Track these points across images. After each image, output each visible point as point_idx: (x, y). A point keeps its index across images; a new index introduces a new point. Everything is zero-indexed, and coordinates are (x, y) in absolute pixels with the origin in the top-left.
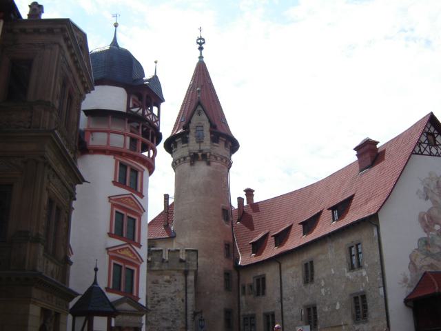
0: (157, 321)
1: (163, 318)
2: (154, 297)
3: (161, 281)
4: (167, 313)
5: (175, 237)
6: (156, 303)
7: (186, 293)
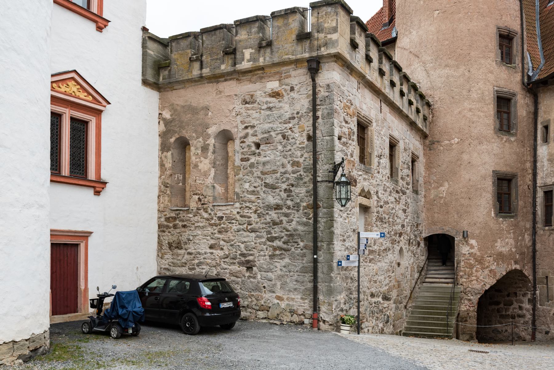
0: (253, 193)
1: (267, 185)
2: (246, 136)
3: (260, 97)
4: (275, 172)
6: (253, 148)
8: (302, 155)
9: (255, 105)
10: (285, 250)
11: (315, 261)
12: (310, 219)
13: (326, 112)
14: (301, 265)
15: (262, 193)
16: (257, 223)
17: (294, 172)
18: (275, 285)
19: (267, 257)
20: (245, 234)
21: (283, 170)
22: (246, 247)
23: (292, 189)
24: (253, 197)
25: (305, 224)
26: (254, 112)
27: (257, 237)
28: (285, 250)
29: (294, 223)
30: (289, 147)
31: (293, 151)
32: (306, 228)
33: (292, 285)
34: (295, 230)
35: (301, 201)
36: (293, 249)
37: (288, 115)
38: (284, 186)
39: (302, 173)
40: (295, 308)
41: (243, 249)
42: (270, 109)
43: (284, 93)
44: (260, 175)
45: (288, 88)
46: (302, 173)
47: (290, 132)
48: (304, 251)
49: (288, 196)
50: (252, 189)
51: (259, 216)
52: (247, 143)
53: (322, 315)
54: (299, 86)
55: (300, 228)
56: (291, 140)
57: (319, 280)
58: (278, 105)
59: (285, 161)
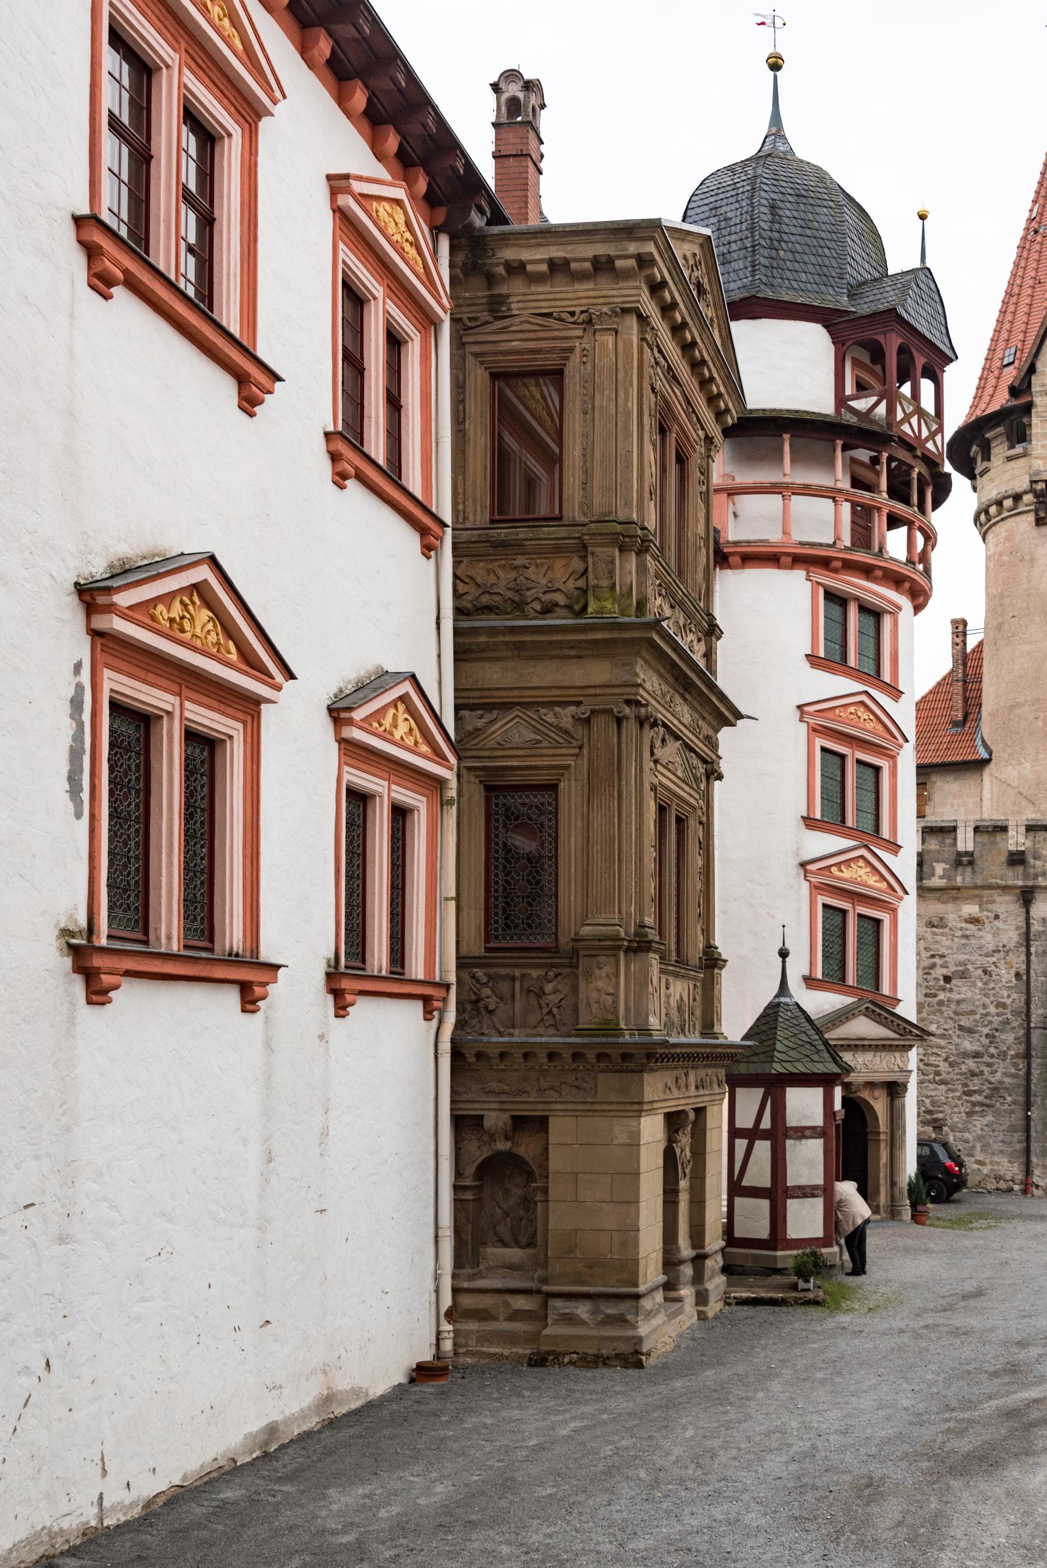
0: (943, 1036)
1: (961, 1028)
2: (933, 966)
3: (952, 919)
4: (972, 1012)
5: (988, 761)
6: (942, 983)
7: (1028, 954)
8: (1009, 996)
9: (946, 930)
10: (988, 1106)
11: (1028, 1119)
12: (1020, 1070)
13: (1041, 949)
14: (1008, 1123)
15: (956, 1039)
16: (948, 1073)
17: (998, 1015)
18: (973, 1147)
19: (963, 1115)
20: (932, 1086)
21: (984, 1012)
22: (933, 1103)
23: (997, 1034)
24: (942, 1042)
25: (1014, 1076)
26: (944, 938)
27: (949, 1090)
28: (988, 1106)
29: (999, 1074)
30: (992, 985)
31: (997, 990)
32: (1014, 1081)
33: (996, 1146)
34: (1001, 1082)
35: (1008, 1049)
36: (998, 1105)
37: (991, 947)
38: (986, 1031)
39: (1009, 1016)
40: (1001, 1173)
41: (929, 1105)
42: (967, 937)
43: (986, 921)
44: (952, 1015)
45: (992, 915)
46: (1009, 1016)
47: (993, 967)
48: (1013, 1107)
49: (991, 1043)
50: (940, 1031)
51: (951, 1065)
52: (934, 975)
53: (1035, 1179)
54: (1005, 915)
55: (1006, 1080)
56: (995, 977)
57: (1032, 1140)
58: (977, 933)
59: (987, 1001)
